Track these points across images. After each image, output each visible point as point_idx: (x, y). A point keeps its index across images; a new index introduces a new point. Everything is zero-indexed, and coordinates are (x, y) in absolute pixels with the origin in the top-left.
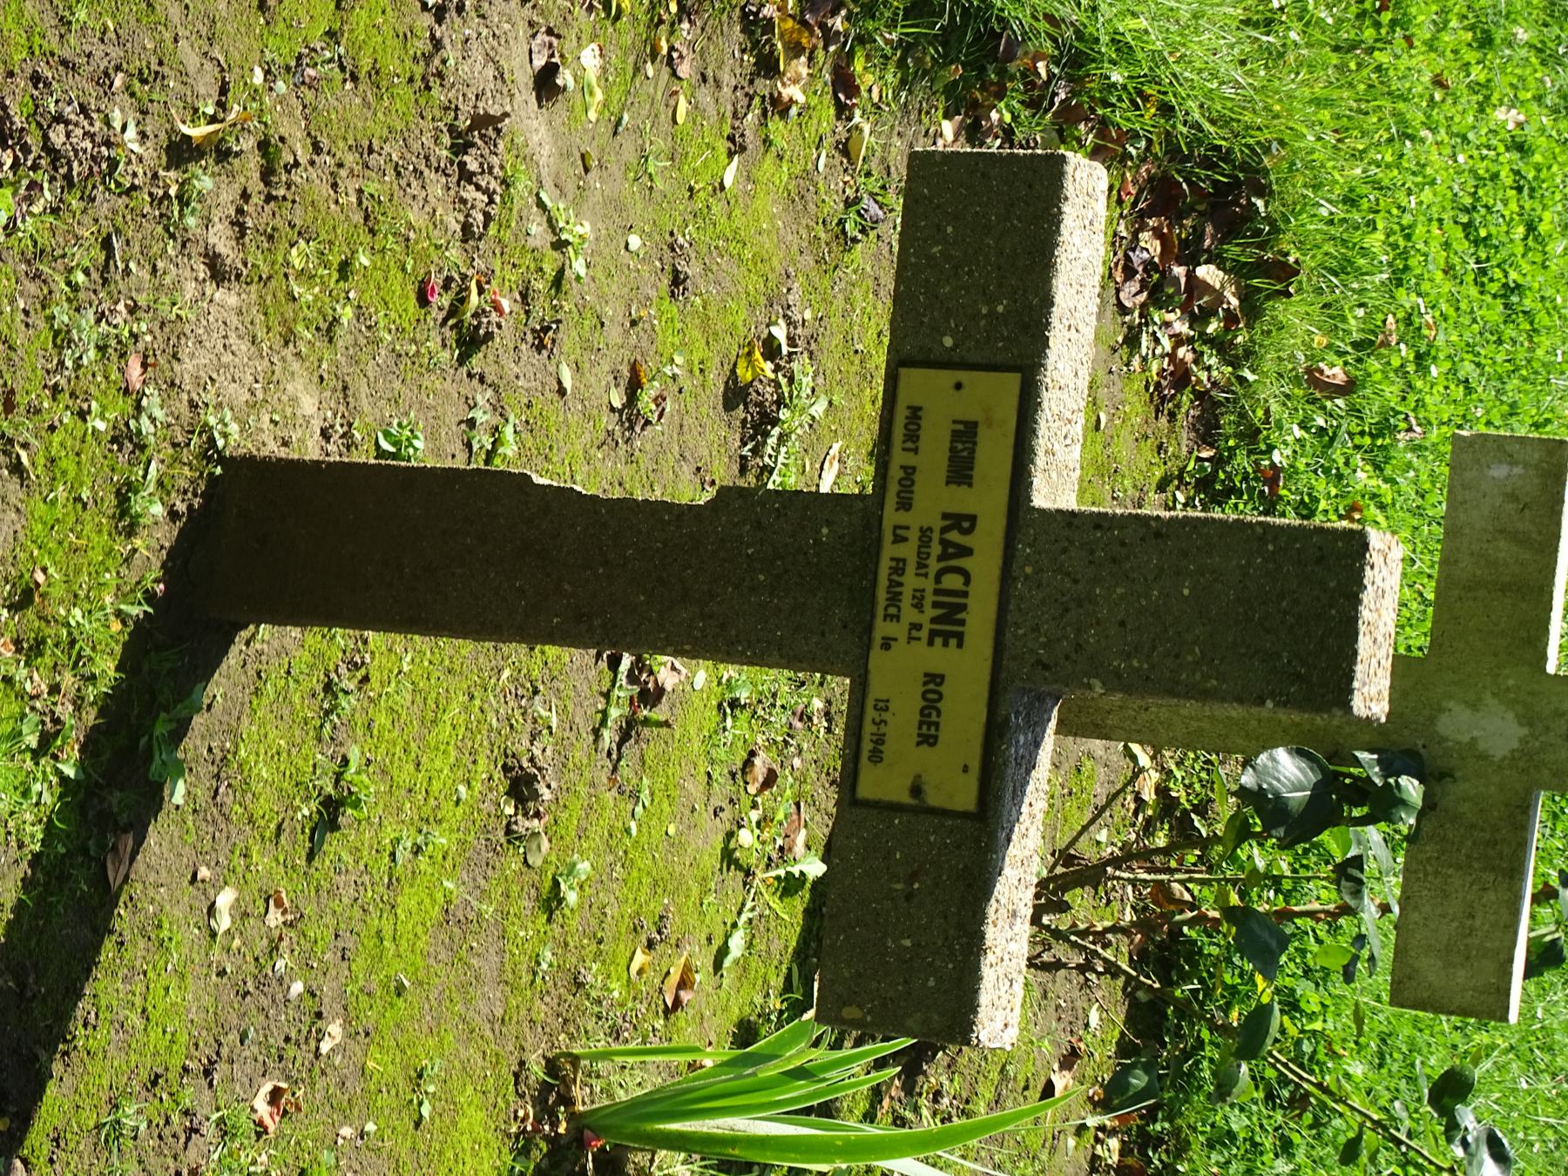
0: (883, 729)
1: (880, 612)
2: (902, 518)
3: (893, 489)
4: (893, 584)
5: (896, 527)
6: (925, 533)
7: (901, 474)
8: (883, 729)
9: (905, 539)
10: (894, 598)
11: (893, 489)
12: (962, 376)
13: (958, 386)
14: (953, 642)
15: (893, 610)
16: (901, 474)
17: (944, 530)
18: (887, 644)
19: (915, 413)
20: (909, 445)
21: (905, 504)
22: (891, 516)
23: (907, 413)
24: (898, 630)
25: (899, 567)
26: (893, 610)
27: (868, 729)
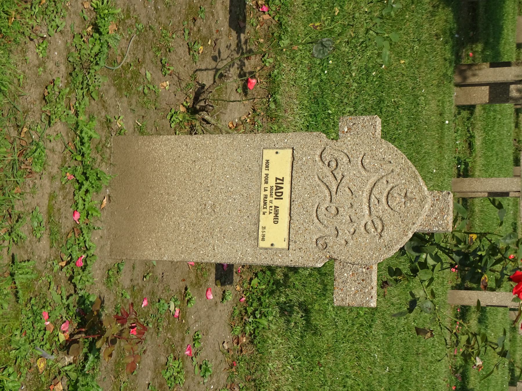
0: (264, 233)
2: (266, 185)
4: (264, 200)
6: (272, 187)
10: (265, 204)
11: (263, 179)
12: (278, 150)
13: (277, 153)
15: (265, 207)
18: (264, 214)
19: (268, 161)
21: (266, 182)
22: (264, 186)
24: (267, 210)
25: (266, 196)
26: (265, 207)
27: (260, 233)
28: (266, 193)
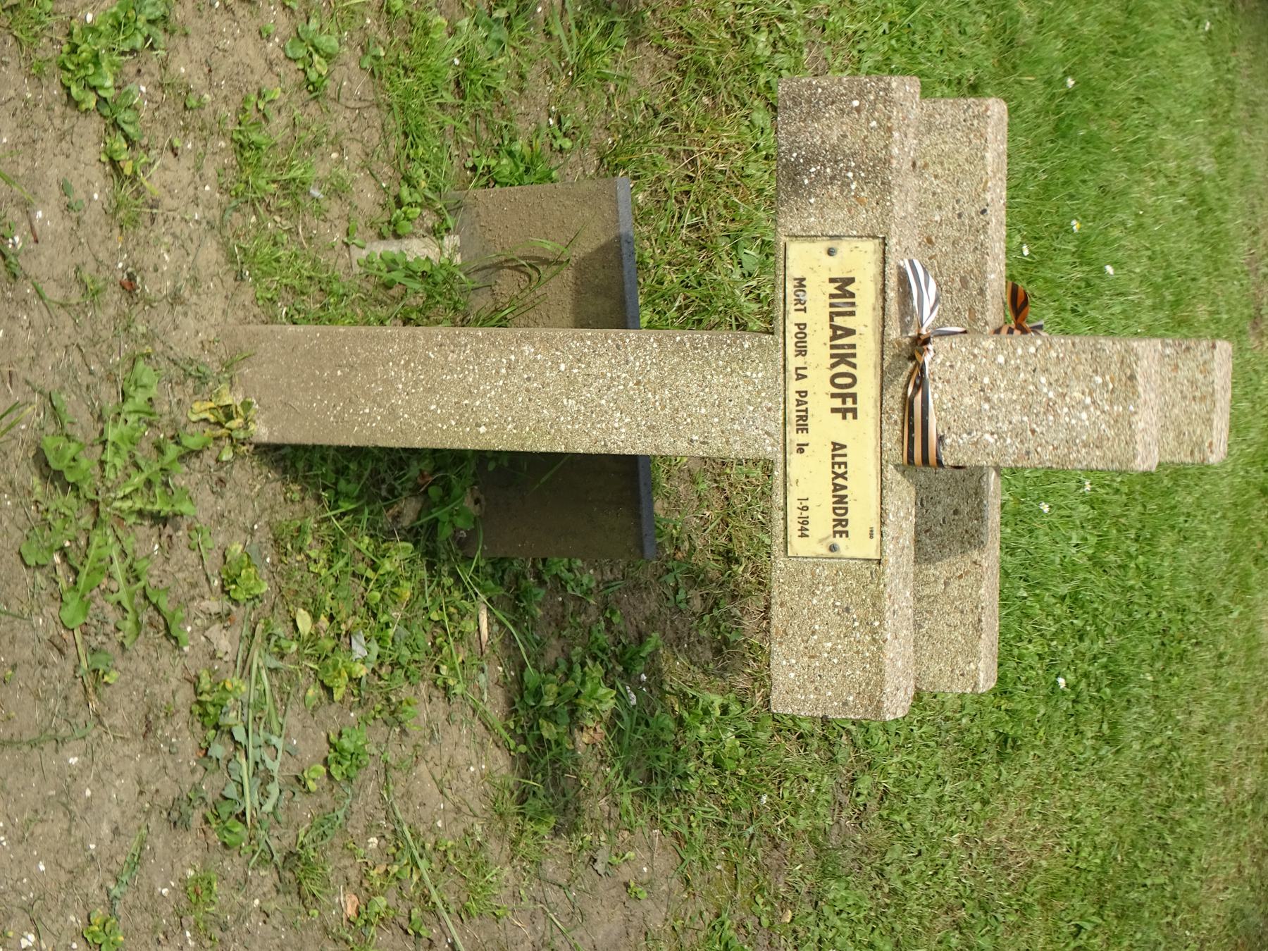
1: (791, 429)
2: (800, 361)
3: (791, 341)
5: (797, 369)
7: (796, 329)
8: (805, 514)
9: (804, 377)
11: (791, 341)
14: (850, 415)
16: (796, 329)
17: (833, 366)
18: (801, 451)
19: (801, 283)
20: (799, 306)
21: (802, 352)
22: (794, 362)
23: (796, 283)
28: (802, 385)
